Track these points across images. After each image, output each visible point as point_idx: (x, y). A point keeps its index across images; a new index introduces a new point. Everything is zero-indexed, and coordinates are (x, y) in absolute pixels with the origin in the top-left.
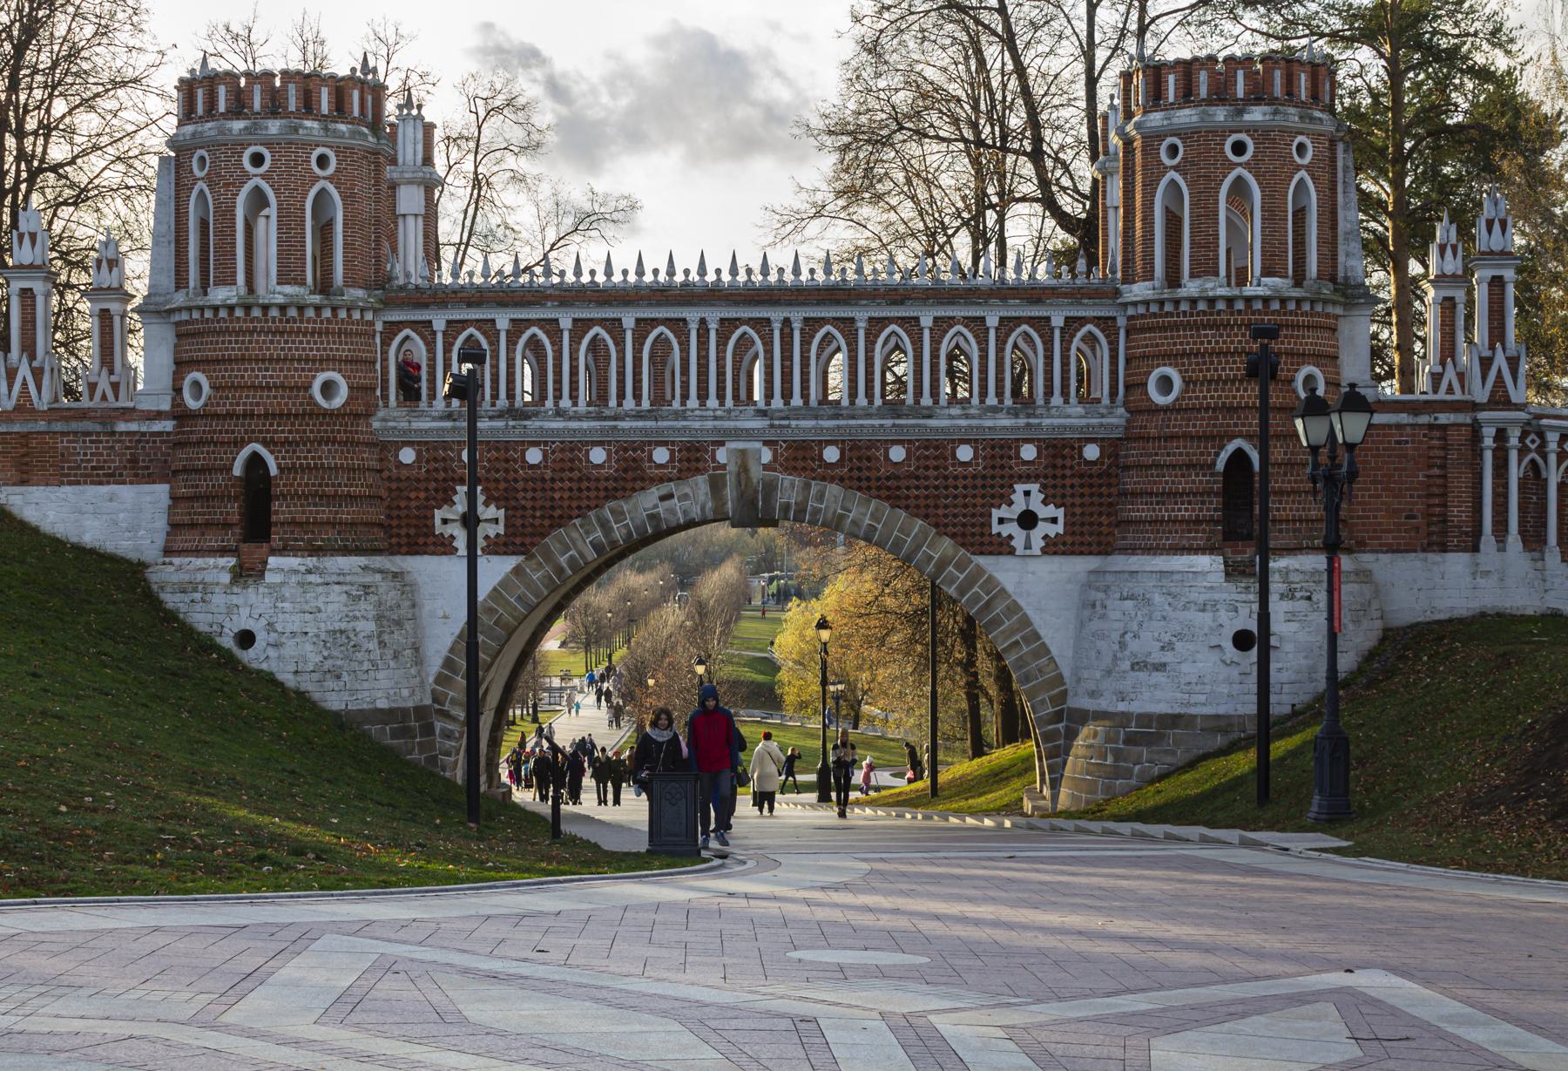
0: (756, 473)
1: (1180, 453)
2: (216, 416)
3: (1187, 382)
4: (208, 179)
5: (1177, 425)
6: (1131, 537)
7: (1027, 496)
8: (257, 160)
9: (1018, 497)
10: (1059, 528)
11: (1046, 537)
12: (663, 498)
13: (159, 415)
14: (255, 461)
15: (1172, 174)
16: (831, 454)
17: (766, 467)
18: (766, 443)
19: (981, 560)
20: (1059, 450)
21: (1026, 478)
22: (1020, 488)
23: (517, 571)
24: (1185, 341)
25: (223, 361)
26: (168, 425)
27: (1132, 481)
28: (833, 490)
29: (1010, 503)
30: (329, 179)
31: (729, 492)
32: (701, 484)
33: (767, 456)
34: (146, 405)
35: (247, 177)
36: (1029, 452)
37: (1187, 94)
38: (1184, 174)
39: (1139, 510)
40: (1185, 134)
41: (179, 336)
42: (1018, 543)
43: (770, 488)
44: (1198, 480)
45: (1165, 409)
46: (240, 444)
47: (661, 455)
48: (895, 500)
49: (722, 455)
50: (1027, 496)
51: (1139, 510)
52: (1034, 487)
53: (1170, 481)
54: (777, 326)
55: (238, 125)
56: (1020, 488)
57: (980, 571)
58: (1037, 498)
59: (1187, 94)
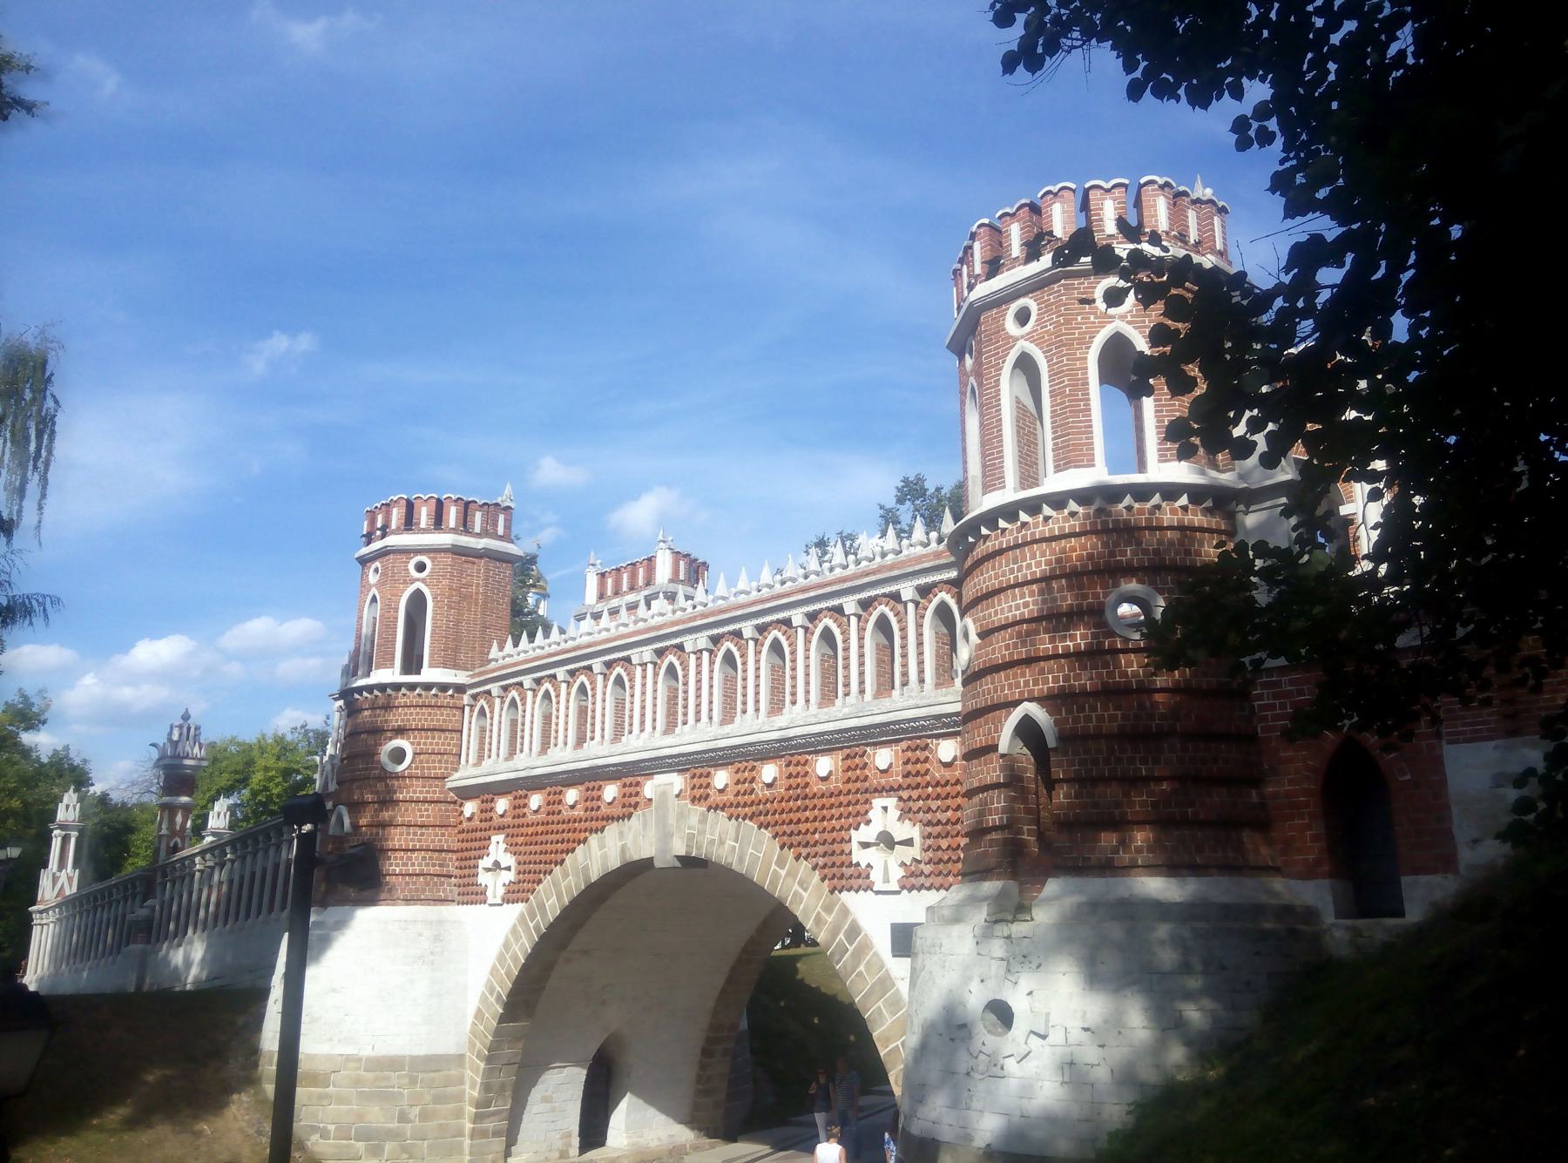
7: (884, 814)
9: (875, 814)
10: (915, 852)
11: (903, 864)
19: (846, 897)
21: (880, 791)
22: (878, 803)
23: (522, 919)
29: (868, 822)
30: (423, 581)
42: (876, 876)
50: (884, 814)
52: (891, 802)
56: (878, 803)
57: (845, 911)
58: (894, 813)
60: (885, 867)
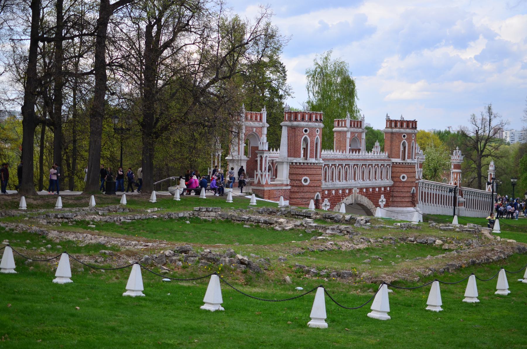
0: (356, 193)
1: (406, 189)
2: (310, 186)
3: (408, 177)
4: (309, 135)
5: (406, 185)
6: (396, 204)
8: (306, 131)
12: (346, 200)
13: (287, 185)
14: (318, 196)
15: (404, 140)
16: (364, 190)
17: (358, 193)
18: (358, 188)
20: (385, 188)
21: (382, 194)
24: (407, 170)
25: (313, 174)
26: (289, 187)
27: (396, 194)
28: (364, 197)
31: (354, 198)
32: (350, 196)
33: (358, 191)
34: (285, 183)
35: (316, 135)
36: (383, 189)
37: (408, 127)
38: (407, 141)
39: (398, 199)
40: (407, 134)
41: (290, 168)
43: (358, 197)
44: (409, 194)
45: (403, 182)
46: (316, 192)
47: (347, 191)
48: (370, 199)
49: (353, 191)
51: (398, 199)
53: (404, 195)
54: (359, 166)
55: (317, 124)
59: (408, 127)
60: (382, 204)
